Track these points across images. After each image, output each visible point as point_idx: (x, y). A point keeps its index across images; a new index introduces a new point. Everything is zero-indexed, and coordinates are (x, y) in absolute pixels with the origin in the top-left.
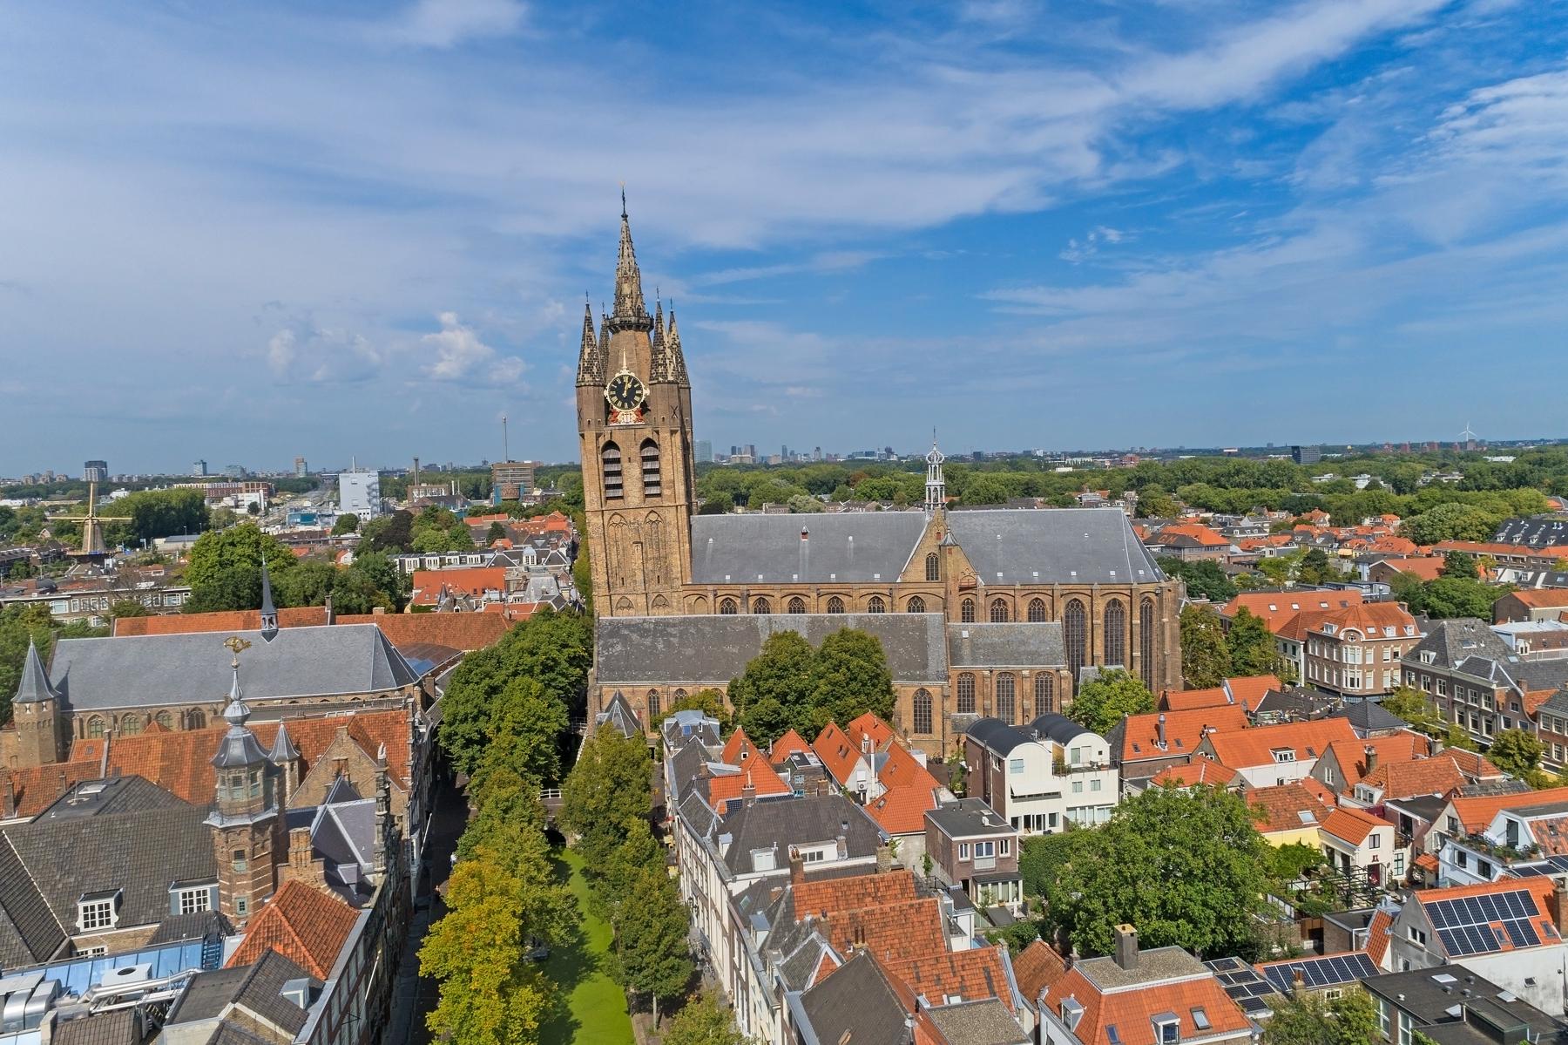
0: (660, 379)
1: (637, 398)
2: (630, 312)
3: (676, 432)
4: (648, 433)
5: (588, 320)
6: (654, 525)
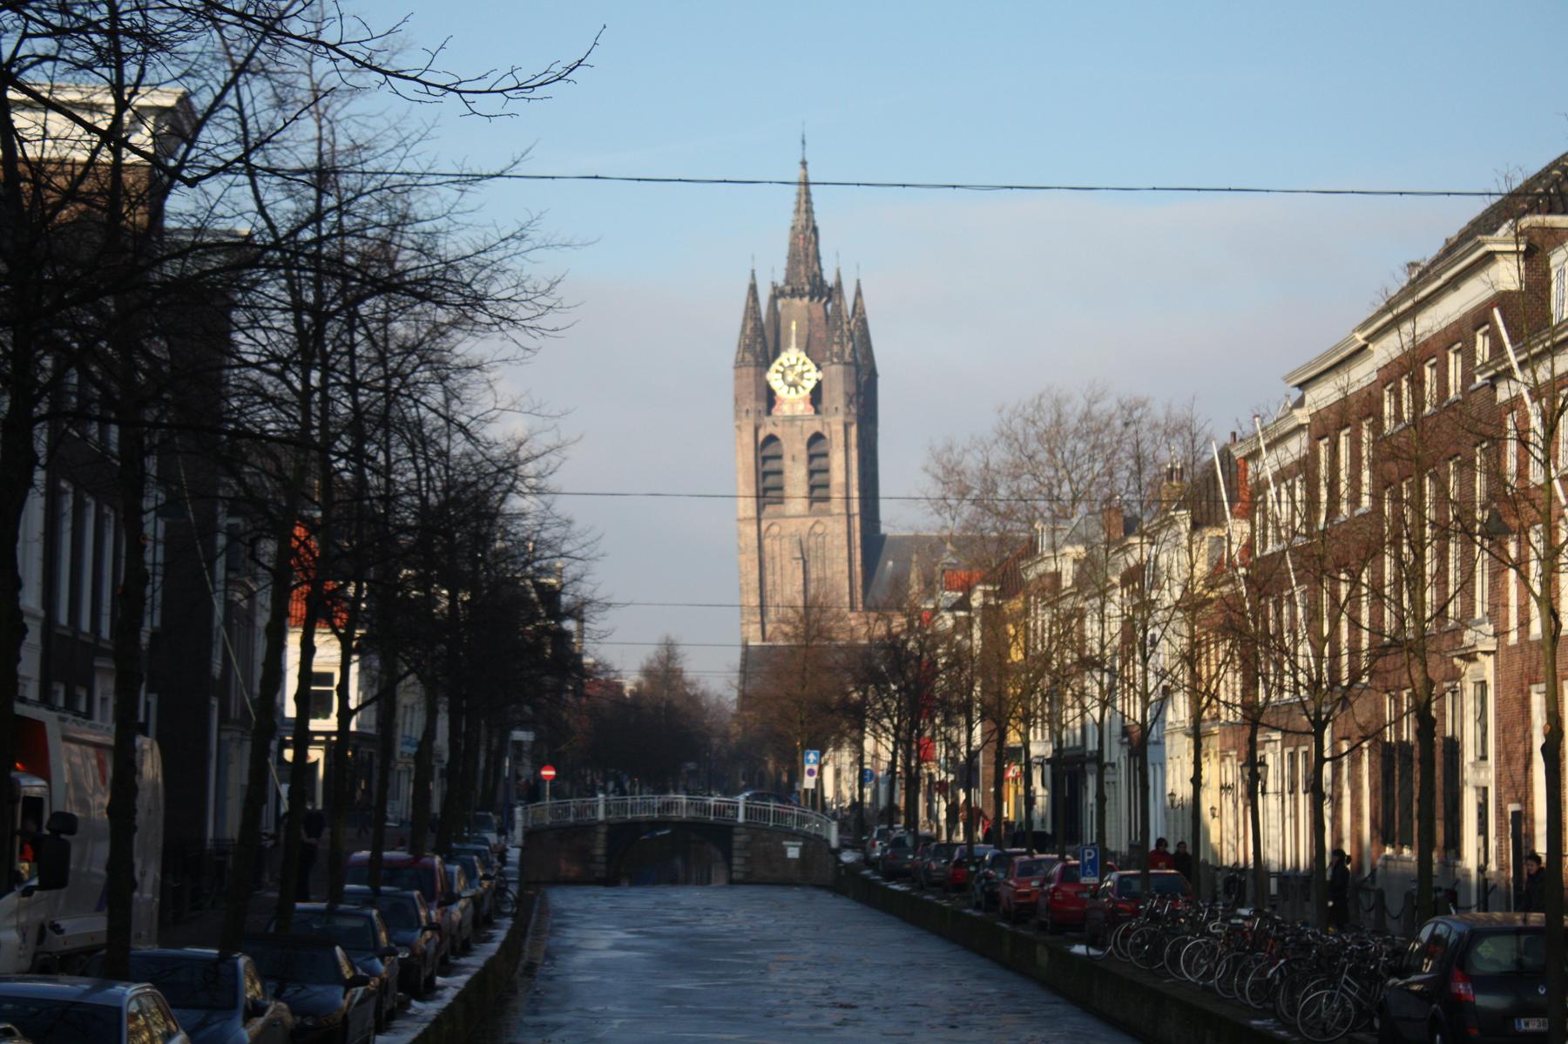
0: (835, 360)
1: (805, 383)
2: (804, 280)
3: (851, 424)
4: (816, 426)
5: (753, 289)
6: (820, 539)
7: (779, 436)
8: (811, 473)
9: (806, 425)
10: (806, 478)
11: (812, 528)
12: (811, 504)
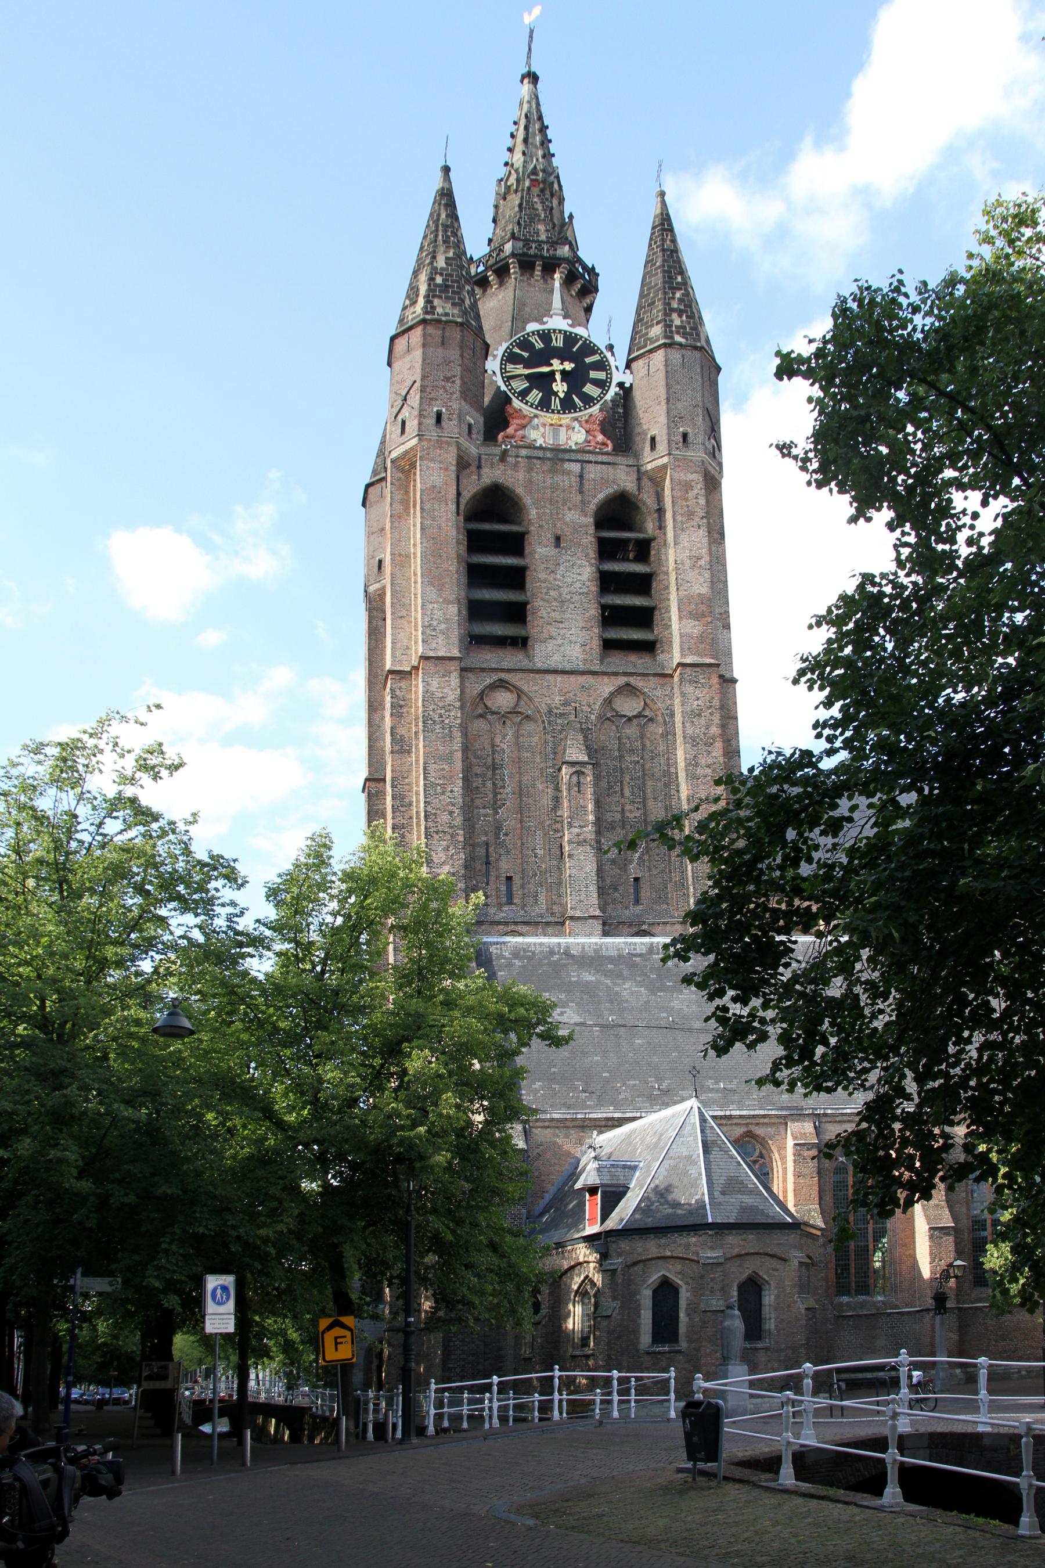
1: (590, 389)
4: (624, 479)
5: (446, 198)
7: (520, 490)
8: (607, 582)
9: (593, 472)
10: (594, 588)
11: (609, 701)
12: (609, 645)
